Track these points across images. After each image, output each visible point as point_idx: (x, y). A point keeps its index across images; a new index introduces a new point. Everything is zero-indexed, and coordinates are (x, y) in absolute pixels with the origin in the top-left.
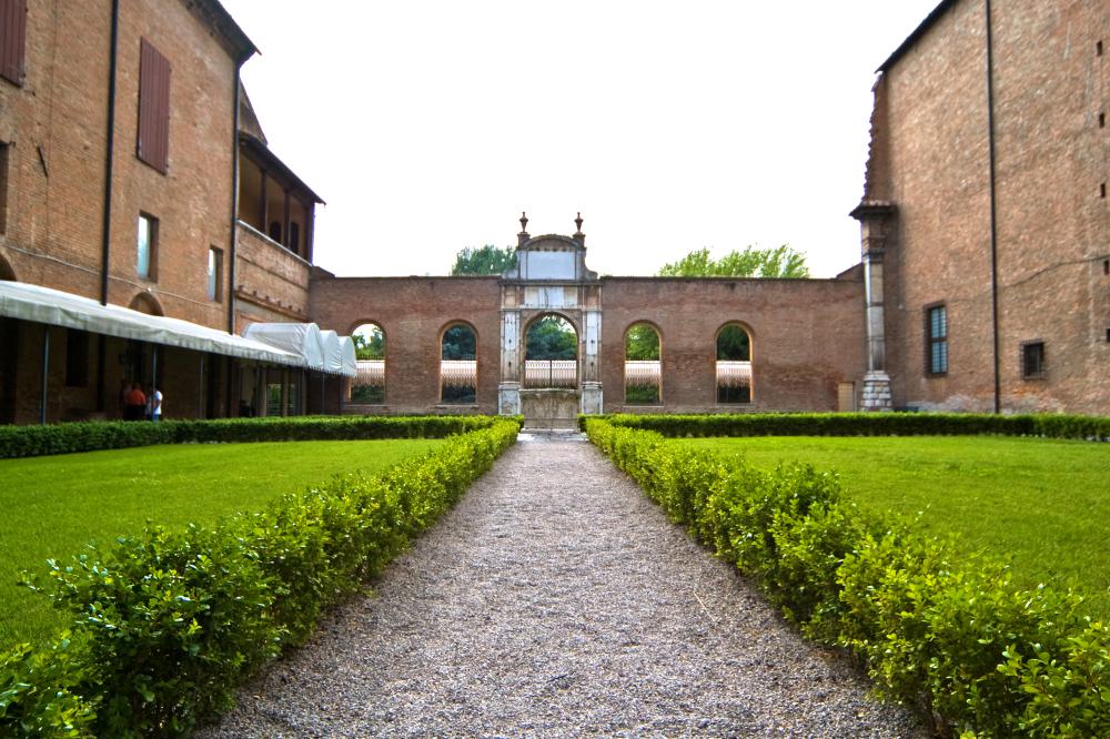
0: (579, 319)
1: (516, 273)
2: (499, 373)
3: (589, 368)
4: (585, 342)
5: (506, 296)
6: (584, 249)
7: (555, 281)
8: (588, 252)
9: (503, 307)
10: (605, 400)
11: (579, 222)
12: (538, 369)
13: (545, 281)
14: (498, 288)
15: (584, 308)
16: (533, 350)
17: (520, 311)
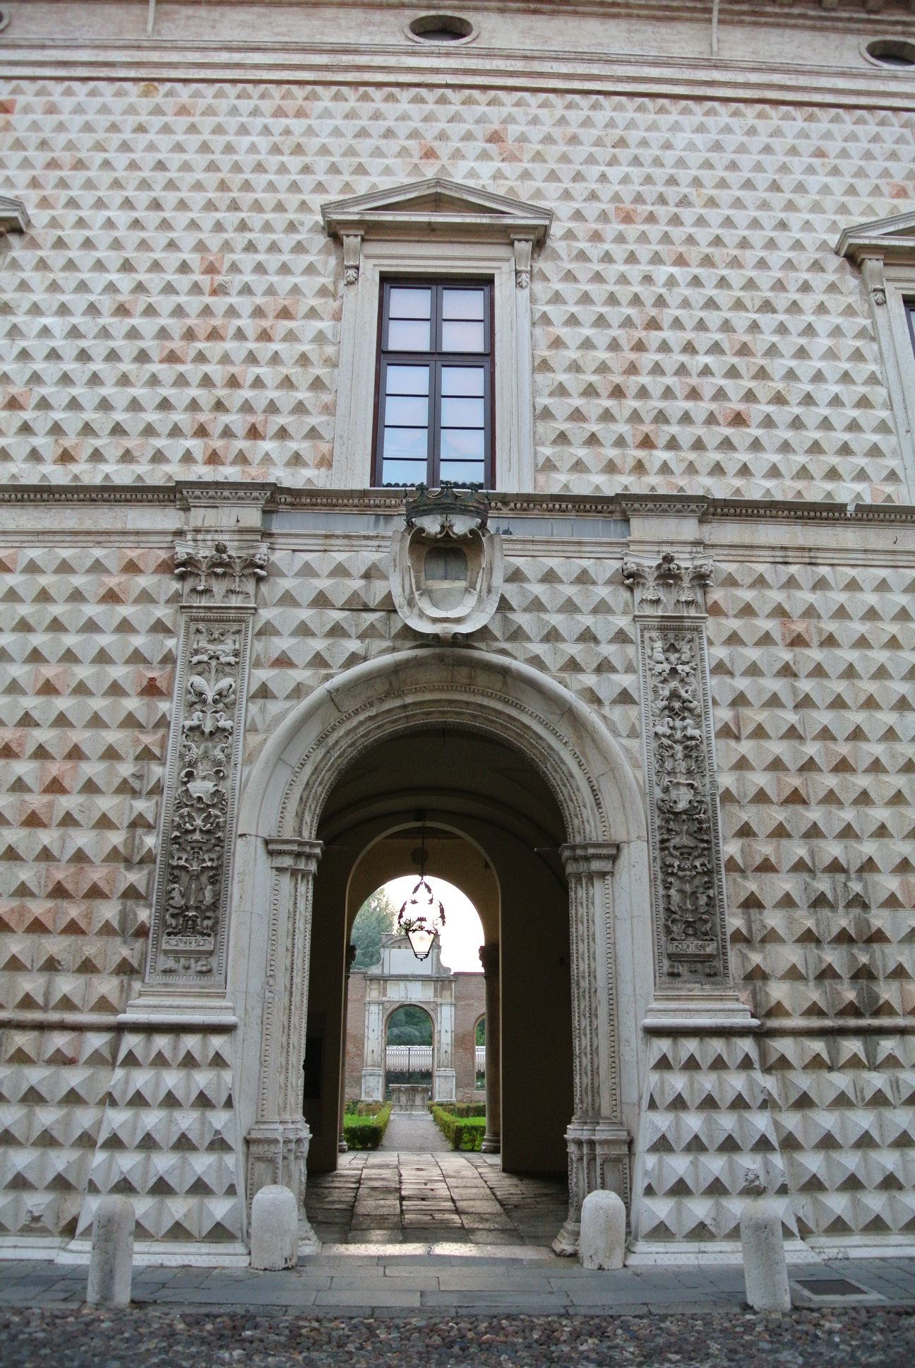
0: (435, 1010)
3: (443, 1056)
10: (457, 1086)
15: (439, 1000)
17: (382, 1003)
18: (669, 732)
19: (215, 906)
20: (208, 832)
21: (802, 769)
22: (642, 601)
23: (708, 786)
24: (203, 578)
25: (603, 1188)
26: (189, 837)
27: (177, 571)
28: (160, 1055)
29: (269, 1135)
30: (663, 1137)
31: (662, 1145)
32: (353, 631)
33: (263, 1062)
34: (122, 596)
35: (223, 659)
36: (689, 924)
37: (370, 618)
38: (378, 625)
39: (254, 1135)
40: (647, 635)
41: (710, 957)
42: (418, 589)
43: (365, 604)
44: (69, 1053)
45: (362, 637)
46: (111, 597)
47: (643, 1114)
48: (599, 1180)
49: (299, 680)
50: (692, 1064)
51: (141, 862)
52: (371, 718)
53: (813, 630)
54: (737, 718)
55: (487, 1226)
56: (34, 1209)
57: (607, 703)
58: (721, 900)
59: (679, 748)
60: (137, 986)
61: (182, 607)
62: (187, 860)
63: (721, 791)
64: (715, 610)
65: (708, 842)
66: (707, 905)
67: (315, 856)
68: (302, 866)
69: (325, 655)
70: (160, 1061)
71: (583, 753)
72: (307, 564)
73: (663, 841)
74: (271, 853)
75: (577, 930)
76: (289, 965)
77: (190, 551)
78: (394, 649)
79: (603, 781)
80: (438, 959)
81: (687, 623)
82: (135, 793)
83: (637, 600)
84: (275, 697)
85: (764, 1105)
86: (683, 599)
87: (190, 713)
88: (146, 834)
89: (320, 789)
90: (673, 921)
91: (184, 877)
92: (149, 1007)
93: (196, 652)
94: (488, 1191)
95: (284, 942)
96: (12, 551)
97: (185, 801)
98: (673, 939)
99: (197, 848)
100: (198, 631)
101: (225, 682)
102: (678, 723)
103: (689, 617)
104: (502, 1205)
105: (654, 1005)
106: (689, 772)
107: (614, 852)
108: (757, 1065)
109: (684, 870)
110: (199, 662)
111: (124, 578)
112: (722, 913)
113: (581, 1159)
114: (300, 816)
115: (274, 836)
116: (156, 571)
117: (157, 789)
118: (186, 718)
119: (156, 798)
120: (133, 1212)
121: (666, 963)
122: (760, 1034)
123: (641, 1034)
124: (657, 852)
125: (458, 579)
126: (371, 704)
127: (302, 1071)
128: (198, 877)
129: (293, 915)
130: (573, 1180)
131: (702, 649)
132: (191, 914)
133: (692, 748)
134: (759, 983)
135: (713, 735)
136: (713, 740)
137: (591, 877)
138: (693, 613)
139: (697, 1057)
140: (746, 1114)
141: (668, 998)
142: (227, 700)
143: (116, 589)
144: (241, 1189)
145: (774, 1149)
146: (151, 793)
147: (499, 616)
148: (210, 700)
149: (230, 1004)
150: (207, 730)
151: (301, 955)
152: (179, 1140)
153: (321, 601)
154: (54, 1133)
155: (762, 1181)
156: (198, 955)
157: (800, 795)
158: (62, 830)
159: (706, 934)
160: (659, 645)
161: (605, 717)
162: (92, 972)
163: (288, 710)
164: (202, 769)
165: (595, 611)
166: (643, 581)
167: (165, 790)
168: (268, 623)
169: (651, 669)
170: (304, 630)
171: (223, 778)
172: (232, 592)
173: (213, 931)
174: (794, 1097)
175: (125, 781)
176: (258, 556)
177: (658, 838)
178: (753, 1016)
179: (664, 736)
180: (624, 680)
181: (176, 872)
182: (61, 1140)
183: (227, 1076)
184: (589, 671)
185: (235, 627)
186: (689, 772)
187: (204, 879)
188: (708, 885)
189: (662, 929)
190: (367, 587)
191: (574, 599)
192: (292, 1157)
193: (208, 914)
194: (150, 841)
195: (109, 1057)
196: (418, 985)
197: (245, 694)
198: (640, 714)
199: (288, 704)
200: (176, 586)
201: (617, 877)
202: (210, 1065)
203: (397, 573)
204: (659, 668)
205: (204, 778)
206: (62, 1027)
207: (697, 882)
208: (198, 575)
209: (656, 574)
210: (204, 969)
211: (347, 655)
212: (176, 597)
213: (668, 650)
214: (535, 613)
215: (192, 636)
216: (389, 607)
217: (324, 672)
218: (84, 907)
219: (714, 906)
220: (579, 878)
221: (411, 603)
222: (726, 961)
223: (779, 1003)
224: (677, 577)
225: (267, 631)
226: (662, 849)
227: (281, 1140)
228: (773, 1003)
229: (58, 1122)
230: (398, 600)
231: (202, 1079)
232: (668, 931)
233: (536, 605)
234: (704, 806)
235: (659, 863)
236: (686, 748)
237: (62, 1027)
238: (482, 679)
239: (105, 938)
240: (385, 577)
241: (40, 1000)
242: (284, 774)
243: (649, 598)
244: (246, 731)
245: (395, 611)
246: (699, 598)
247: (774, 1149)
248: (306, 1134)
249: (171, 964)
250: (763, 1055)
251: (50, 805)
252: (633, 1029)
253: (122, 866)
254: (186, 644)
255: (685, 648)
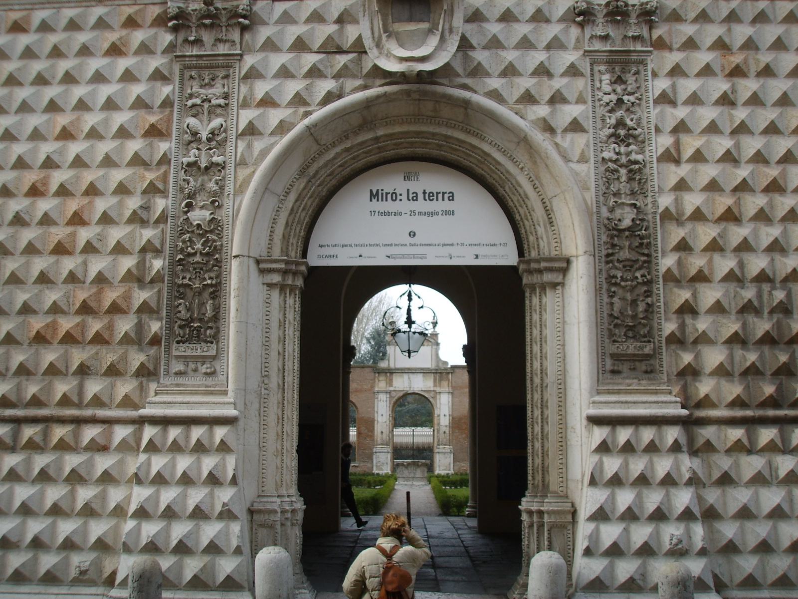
1: (387, 362)
2: (373, 440)
3: (442, 436)
4: (439, 416)
5: (379, 381)
6: (438, 344)
7: (416, 369)
8: (441, 346)
9: (376, 389)
10: (455, 461)
11: (435, 324)
12: (406, 435)
13: (409, 369)
14: (373, 374)
15: (438, 389)
16: (398, 421)
17: (390, 392)
18: (614, 157)
19: (216, 318)
20: (208, 254)
21: (736, 190)
22: (592, 37)
23: (650, 205)
24: (194, 29)
25: (550, 548)
26: (191, 260)
27: (170, 24)
28: (175, 442)
29: (269, 507)
30: (601, 508)
31: (601, 515)
32: (329, 72)
33: (262, 448)
34: (123, 49)
35: (214, 102)
36: (631, 328)
37: (342, 60)
38: (351, 66)
39: (257, 506)
40: (596, 68)
41: (648, 357)
42: (384, 33)
43: (338, 47)
44: (102, 441)
45: (337, 76)
46: (115, 50)
47: (585, 489)
48: (546, 543)
49: (281, 117)
50: (628, 448)
51: (152, 281)
52: (347, 150)
53: (751, 62)
54: (677, 144)
55: (456, 578)
56: (82, 565)
57: (559, 131)
58: (659, 307)
59: (623, 171)
60: (153, 386)
61: (176, 57)
62: (190, 279)
63: (660, 210)
64: (661, 44)
65: (648, 255)
66: (646, 311)
67: (301, 273)
68: (290, 282)
69: (305, 95)
70: (176, 448)
71: (538, 178)
72: (285, 13)
73: (608, 255)
74: (262, 271)
75: (532, 333)
76: (281, 367)
77: (181, 5)
78: (365, 87)
79: (555, 202)
80: (437, 355)
81: (634, 57)
82: (144, 223)
83: (587, 36)
84: (261, 134)
85: (690, 482)
86: (630, 34)
87: (188, 151)
88: (155, 258)
89: (303, 214)
90: (616, 326)
91: (190, 294)
92: (164, 403)
93: (191, 96)
94: (463, 549)
95: (275, 346)
96: (24, 13)
97: (186, 227)
98: (614, 341)
99: (200, 269)
100: (191, 77)
101: (216, 122)
102: (623, 149)
103: (635, 51)
104: (472, 561)
105: (597, 398)
106: (633, 193)
107: (565, 265)
108: (685, 449)
109: (627, 280)
110: (194, 106)
111: (124, 32)
112: (659, 318)
113: (531, 526)
114: (285, 238)
115: (264, 254)
116: (152, 25)
117: (162, 219)
118: (184, 156)
119: (162, 226)
120: (160, 569)
121: (609, 363)
122: (688, 423)
123: (585, 422)
124: (603, 264)
125: (421, 20)
126: (347, 138)
127: (295, 454)
128: (200, 294)
129: (282, 324)
130: (525, 542)
131: (646, 80)
132: (196, 325)
133: (636, 171)
134: (689, 379)
135: (655, 159)
136: (655, 165)
137: (543, 288)
138: (639, 48)
139: (633, 442)
140: (673, 491)
141: (609, 392)
142: (219, 138)
143: (118, 43)
144: (246, 549)
145: (697, 519)
146: (157, 222)
147: (460, 54)
148: (204, 138)
149: (232, 400)
150: (203, 165)
151: (291, 358)
152: (194, 510)
153: (300, 45)
154: (93, 505)
155: (684, 544)
156: (203, 359)
157: (733, 213)
158: (84, 256)
159: (645, 336)
160: (606, 78)
161: (557, 145)
162: (116, 375)
163: (272, 146)
164: (201, 200)
165: (548, 47)
166: (593, 18)
167: (169, 219)
168: (252, 68)
169: (600, 100)
170: (285, 73)
171: (219, 207)
172: (219, 40)
173: (216, 338)
174: (716, 475)
175: (134, 212)
176: (241, 7)
177: (604, 252)
178: (683, 407)
179: (611, 160)
180: (572, 111)
181: (181, 290)
182: (99, 511)
183: (231, 462)
184: (543, 102)
185: (222, 73)
186: (633, 193)
187: (206, 295)
188: (648, 293)
189: (606, 333)
190: (341, 31)
191: (530, 37)
192: (289, 524)
193: (210, 324)
194: (157, 264)
195: (134, 445)
196: (420, 377)
197: (234, 132)
198: (588, 141)
199: (273, 139)
200: (168, 38)
201: (567, 287)
202: (217, 450)
203: (367, 18)
204: (606, 99)
205: (202, 208)
206: (93, 421)
207: (637, 291)
208: (189, 27)
209: (605, 11)
210: (208, 371)
211: (323, 93)
212: (171, 48)
213: (615, 82)
214: (494, 51)
215: (186, 82)
216: (359, 48)
217: (302, 110)
218: (106, 321)
219: (652, 312)
220: (533, 288)
221: (378, 45)
222: (661, 360)
223: (707, 396)
224: (625, 14)
225: (253, 74)
226: (607, 263)
227: (279, 510)
228: (702, 394)
229: (95, 496)
230: (368, 43)
231: (208, 463)
232: (611, 334)
233: (495, 44)
234: (645, 224)
235: (604, 275)
236: (630, 171)
237: (93, 421)
238: (446, 112)
239: (124, 346)
240: (355, 21)
241: (75, 399)
242: (271, 202)
243: (599, 34)
244: (236, 165)
245: (366, 52)
246: (645, 34)
247: (697, 519)
248: (300, 505)
249: (180, 367)
250: (691, 440)
251: (73, 235)
252: (578, 418)
253: (136, 285)
254: (182, 89)
255: (631, 79)
